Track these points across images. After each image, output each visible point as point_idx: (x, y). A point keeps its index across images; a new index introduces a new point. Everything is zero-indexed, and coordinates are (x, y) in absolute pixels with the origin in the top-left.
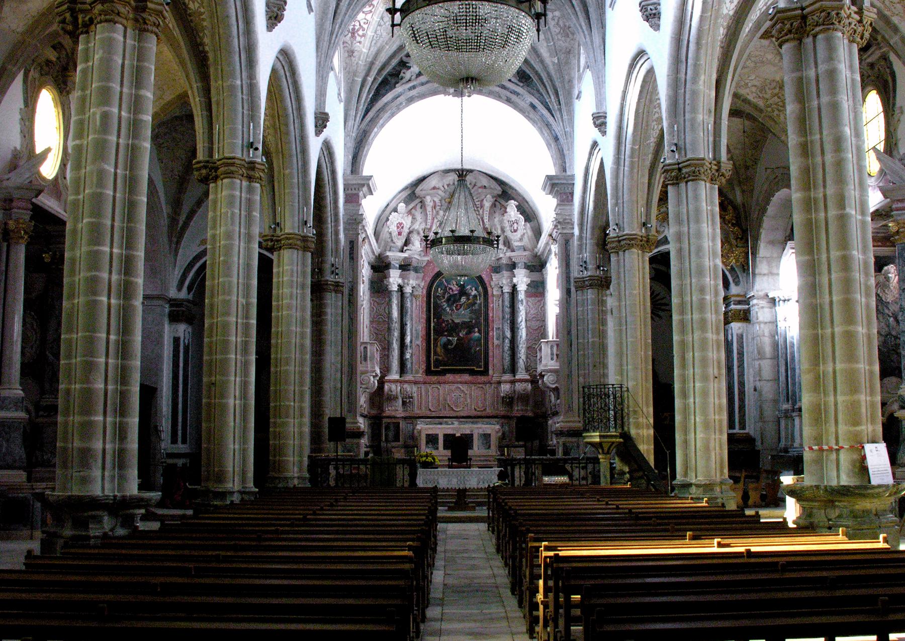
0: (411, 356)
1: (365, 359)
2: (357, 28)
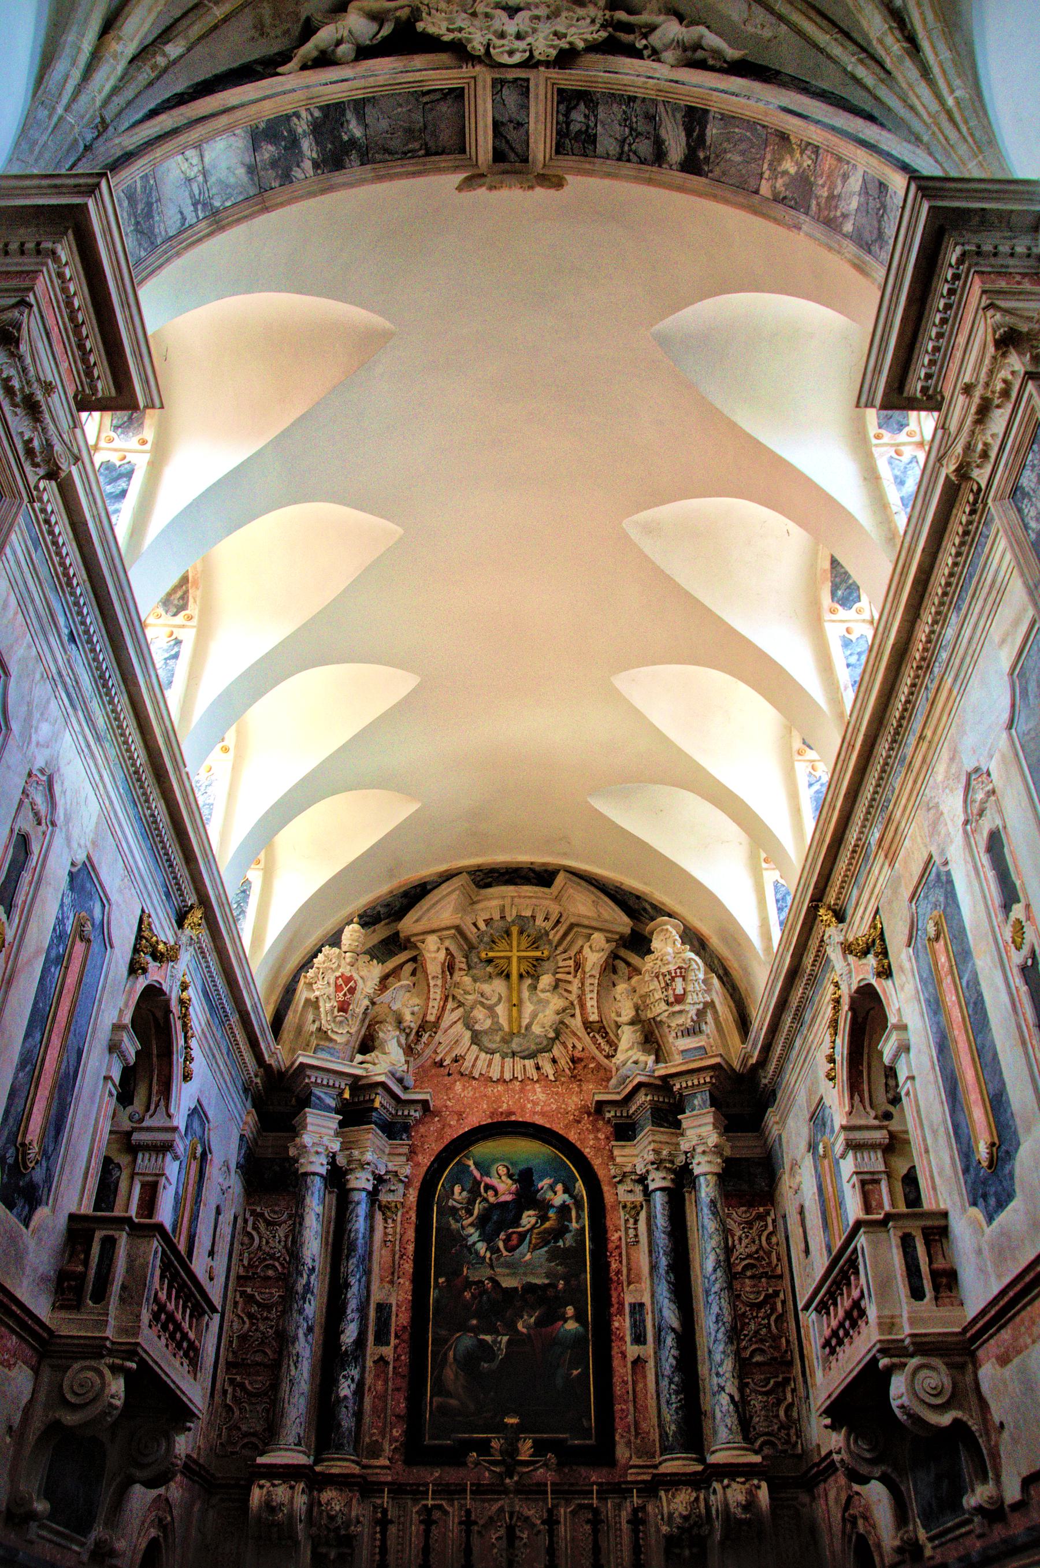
0: (359, 1392)
1: (100, 1295)
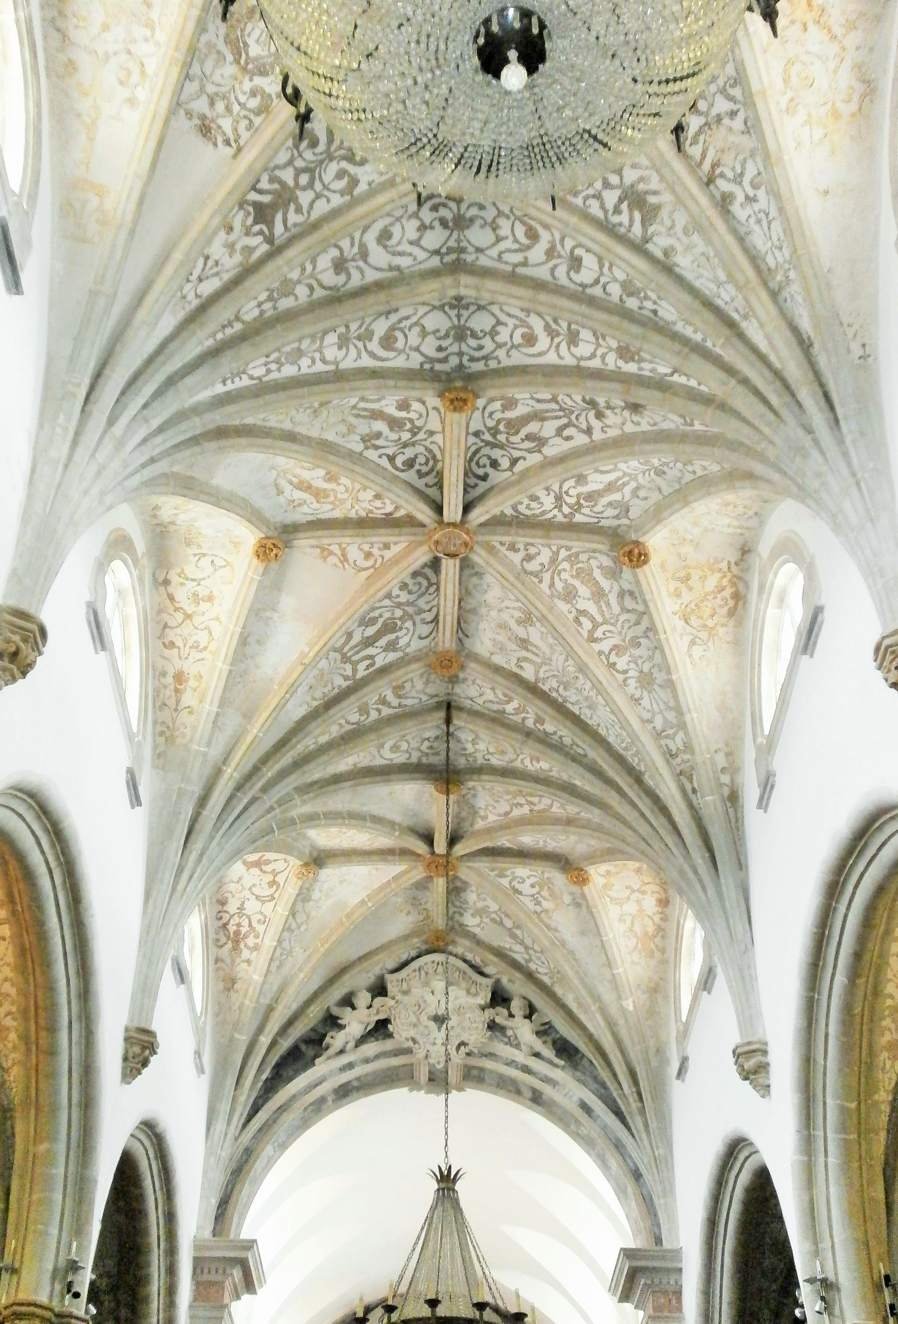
2: (244, 930)
